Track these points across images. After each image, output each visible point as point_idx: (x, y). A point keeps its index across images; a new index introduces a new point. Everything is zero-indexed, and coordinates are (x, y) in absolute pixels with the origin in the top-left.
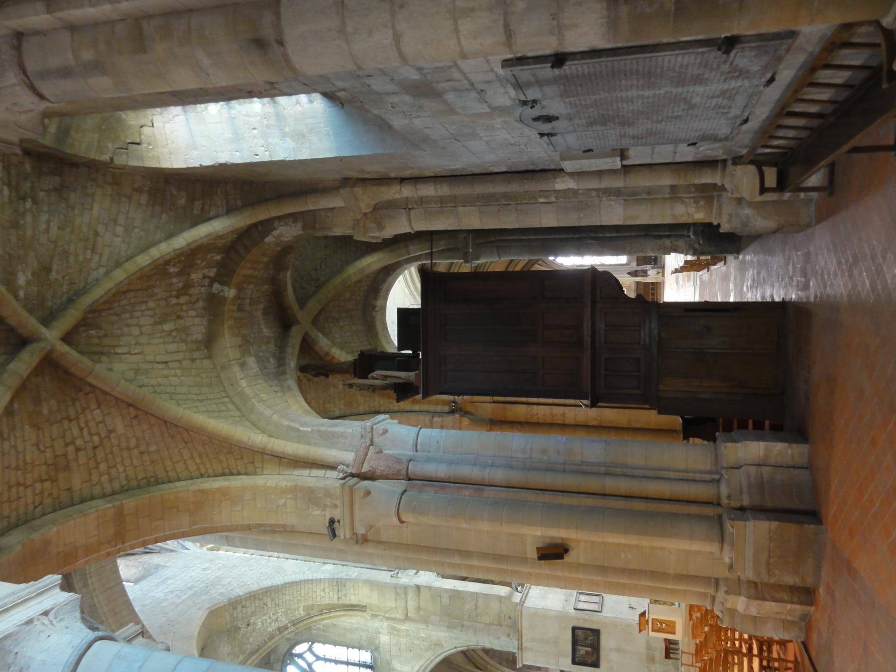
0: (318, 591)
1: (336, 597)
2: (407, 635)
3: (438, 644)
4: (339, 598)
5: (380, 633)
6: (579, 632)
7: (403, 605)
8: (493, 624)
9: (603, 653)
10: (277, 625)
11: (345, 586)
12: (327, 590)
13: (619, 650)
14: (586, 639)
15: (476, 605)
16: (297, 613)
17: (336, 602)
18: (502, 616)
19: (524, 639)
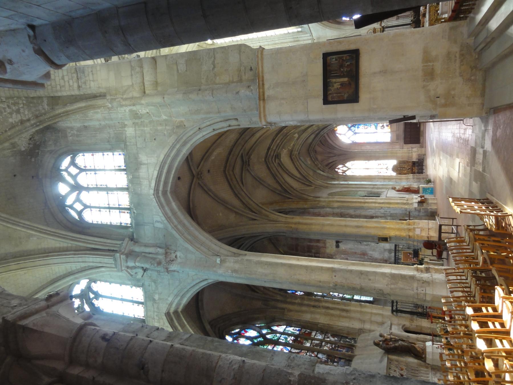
0: (57, 79)
1: (76, 85)
2: (150, 122)
3: (181, 126)
4: (79, 87)
5: (125, 126)
6: (333, 60)
7: (139, 80)
8: (233, 82)
9: (363, 81)
10: (19, 117)
11: (83, 72)
12: (66, 78)
13: (384, 72)
14: (341, 66)
15: (213, 63)
16: (40, 108)
17: (76, 92)
18: (242, 68)
19: (266, 86)
